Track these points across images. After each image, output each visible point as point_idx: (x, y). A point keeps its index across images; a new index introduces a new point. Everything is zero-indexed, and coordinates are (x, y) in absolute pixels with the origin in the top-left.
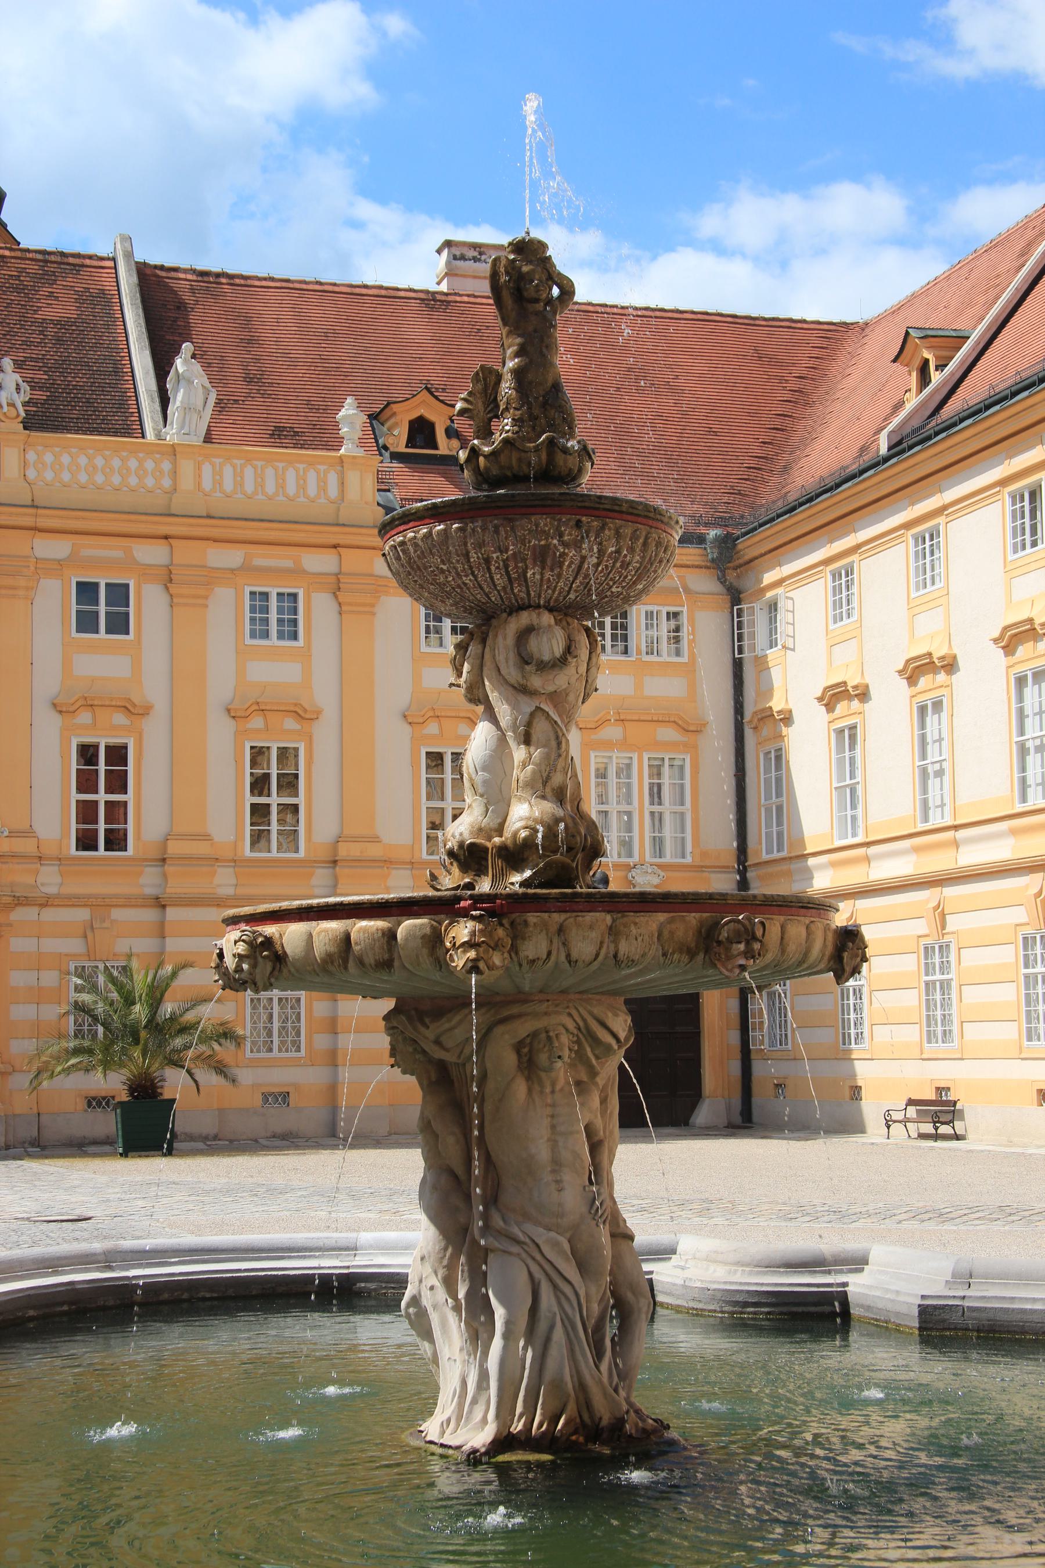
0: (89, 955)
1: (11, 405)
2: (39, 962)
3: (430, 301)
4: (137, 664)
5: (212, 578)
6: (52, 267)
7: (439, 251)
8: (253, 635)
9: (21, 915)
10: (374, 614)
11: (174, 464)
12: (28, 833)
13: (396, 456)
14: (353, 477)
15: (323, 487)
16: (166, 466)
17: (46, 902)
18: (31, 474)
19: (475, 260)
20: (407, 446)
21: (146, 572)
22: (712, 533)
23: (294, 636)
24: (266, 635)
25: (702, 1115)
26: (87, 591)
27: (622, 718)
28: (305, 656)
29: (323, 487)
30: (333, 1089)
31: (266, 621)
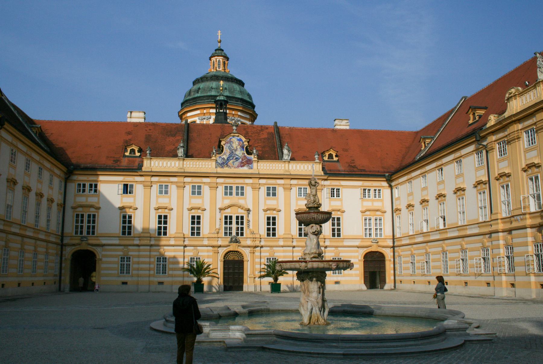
0: (270, 256)
6: (263, 128)
12: (258, 233)
20: (328, 159)
22: (387, 174)
25: (386, 287)
26: (268, 189)
31: (301, 193)
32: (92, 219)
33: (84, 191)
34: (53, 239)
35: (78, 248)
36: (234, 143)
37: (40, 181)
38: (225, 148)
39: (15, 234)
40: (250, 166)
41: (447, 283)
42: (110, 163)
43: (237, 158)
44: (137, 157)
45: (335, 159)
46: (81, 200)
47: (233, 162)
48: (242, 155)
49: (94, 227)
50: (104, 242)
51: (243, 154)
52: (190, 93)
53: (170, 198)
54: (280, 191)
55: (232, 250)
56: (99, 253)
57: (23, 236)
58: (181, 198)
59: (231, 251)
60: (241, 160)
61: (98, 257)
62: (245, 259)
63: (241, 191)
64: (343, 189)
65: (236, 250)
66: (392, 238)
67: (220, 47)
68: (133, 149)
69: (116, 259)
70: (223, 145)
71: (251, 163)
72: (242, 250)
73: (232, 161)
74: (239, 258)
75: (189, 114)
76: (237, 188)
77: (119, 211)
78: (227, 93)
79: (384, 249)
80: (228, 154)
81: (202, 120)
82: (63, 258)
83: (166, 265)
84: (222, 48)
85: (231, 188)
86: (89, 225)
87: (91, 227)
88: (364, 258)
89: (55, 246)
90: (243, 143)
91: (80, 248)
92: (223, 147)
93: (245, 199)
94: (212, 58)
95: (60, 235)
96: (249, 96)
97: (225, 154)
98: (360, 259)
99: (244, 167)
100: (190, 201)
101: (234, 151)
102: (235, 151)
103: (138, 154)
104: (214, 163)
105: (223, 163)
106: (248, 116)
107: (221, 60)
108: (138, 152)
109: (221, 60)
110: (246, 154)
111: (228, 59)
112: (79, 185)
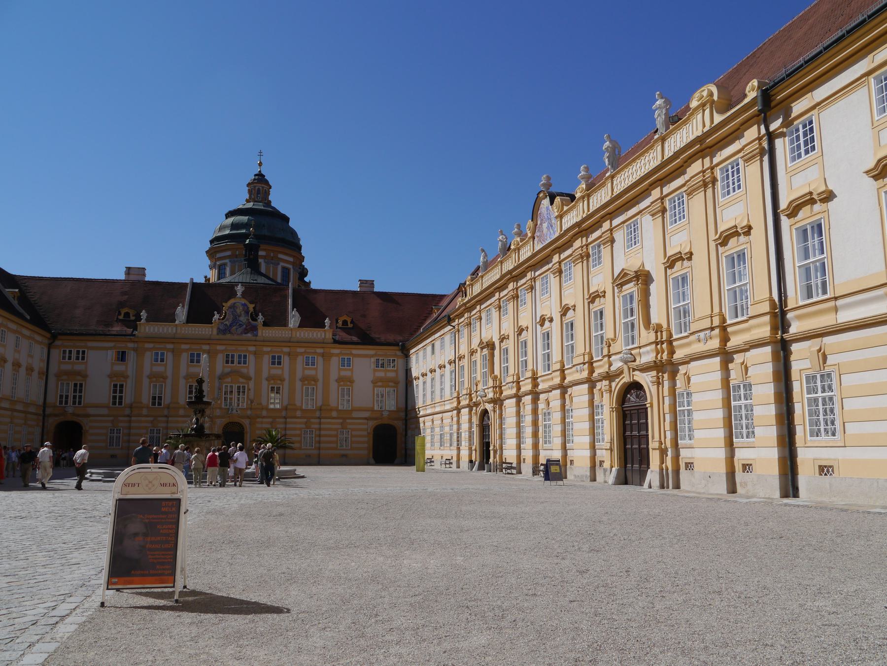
1: (260, 322)
3: (354, 293)
8: (306, 365)
9: (259, 420)
11: (292, 332)
12: (261, 404)
13: (340, 328)
15: (321, 335)
16: (290, 332)
17: (264, 417)
18: (264, 335)
19: (365, 283)
23: (314, 365)
24: (309, 365)
26: (273, 357)
28: (316, 369)
29: (321, 335)
30: (319, 455)
32: (79, 388)
33: (70, 358)
36: (238, 309)
40: (255, 332)
41: (524, 459)
43: (240, 324)
45: (350, 325)
46: (66, 367)
49: (80, 397)
50: (91, 411)
51: (247, 320)
52: (222, 228)
53: (165, 366)
54: (286, 360)
55: (231, 421)
59: (230, 423)
60: (244, 326)
61: (84, 428)
63: (243, 359)
64: (354, 358)
67: (260, 171)
68: (127, 312)
75: (218, 255)
76: (240, 356)
79: (396, 422)
80: (231, 320)
84: (263, 172)
85: (233, 356)
86: (75, 394)
87: (78, 396)
90: (248, 308)
93: (248, 368)
96: (293, 233)
97: (228, 320)
101: (237, 316)
102: (239, 317)
103: (132, 318)
104: (215, 331)
105: (226, 330)
106: (291, 259)
107: (261, 188)
108: (133, 316)
109: (261, 188)
110: (250, 320)
111: (270, 187)
112: (64, 352)
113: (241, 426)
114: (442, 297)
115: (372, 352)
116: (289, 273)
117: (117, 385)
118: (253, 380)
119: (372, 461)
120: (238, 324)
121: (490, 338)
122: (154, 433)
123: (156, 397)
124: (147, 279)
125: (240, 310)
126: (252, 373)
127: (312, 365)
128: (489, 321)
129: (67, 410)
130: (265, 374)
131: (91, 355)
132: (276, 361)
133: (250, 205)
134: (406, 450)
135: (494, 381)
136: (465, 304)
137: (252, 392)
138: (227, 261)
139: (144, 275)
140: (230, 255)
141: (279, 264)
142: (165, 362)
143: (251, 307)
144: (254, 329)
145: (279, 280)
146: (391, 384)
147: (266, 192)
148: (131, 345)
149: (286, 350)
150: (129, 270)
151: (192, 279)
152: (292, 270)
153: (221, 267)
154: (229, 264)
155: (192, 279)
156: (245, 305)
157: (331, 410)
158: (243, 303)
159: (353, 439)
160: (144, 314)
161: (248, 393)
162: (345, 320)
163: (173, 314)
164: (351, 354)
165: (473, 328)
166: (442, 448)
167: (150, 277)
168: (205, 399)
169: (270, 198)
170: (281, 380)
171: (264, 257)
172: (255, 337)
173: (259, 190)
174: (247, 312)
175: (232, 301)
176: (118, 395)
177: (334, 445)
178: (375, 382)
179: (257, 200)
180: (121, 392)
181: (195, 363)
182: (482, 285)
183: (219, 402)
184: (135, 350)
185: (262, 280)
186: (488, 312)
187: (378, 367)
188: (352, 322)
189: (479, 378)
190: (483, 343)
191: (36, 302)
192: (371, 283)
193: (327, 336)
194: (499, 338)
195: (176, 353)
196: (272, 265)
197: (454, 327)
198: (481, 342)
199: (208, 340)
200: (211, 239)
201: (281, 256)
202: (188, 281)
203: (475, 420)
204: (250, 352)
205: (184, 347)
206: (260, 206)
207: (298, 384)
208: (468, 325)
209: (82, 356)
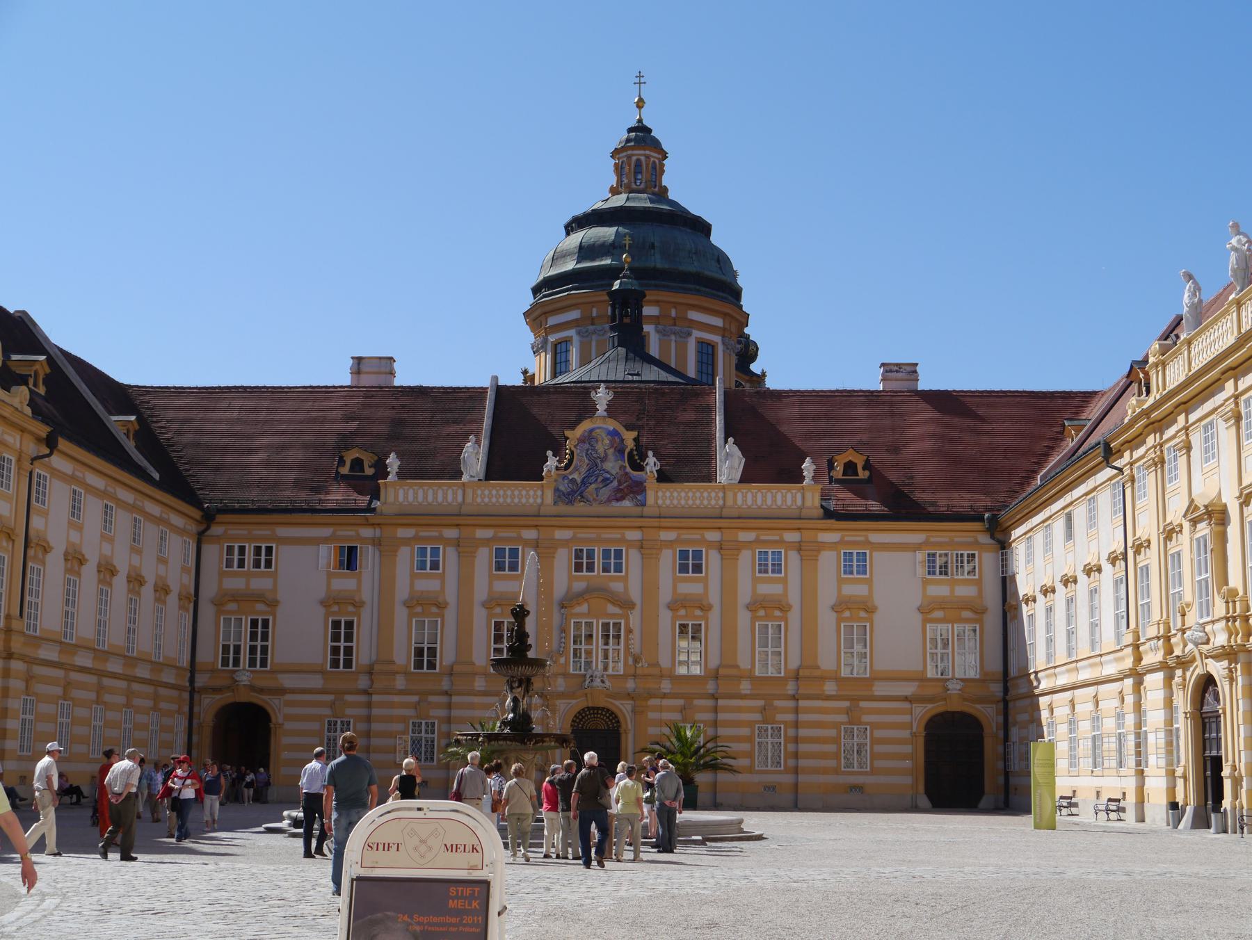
1: (652, 472)
2: (661, 723)
3: (870, 395)
4: (706, 588)
5: (739, 546)
7: (880, 367)
8: (760, 572)
9: (654, 702)
10: (817, 560)
12: (657, 665)
13: (838, 481)
14: (808, 495)
16: (721, 495)
17: (664, 696)
19: (897, 371)
21: (710, 545)
23: (780, 572)
24: (766, 572)
25: (982, 804)
26: (684, 555)
27: (942, 607)
28: (784, 581)
29: (794, 499)
30: (796, 785)
32: (260, 629)
33: (241, 564)
34: (168, 677)
35: (227, 698)
36: (600, 442)
37: (136, 550)
38: (578, 455)
39: (83, 670)
42: (303, 497)
43: (605, 480)
44: (368, 477)
45: (863, 474)
47: (596, 489)
48: (618, 470)
49: (264, 650)
50: (287, 681)
52: (557, 258)
53: (442, 577)
54: (712, 561)
55: (590, 705)
56: (277, 711)
57: (101, 674)
58: (465, 582)
60: (615, 483)
61: (273, 720)
62: (622, 730)
63: (614, 560)
64: (877, 556)
65: (601, 705)
66: (1000, 677)
67: (640, 121)
69: (315, 726)
70: (573, 449)
71: (642, 491)
72: (614, 705)
73: (593, 486)
74: (608, 726)
75: (553, 320)
76: (606, 553)
77: (322, 610)
78: (657, 261)
79: (978, 706)
80: (584, 469)
81: (587, 336)
82: (195, 721)
83: (433, 741)
85: (590, 554)
88: (925, 730)
89: (174, 693)
90: (622, 440)
91: (231, 700)
92: (572, 453)
94: (619, 154)
95: (189, 668)
96: (721, 260)
97: (576, 469)
98: (914, 730)
99: (624, 501)
100: (490, 585)
101: (599, 461)
102: (602, 461)
103: (369, 471)
104: (549, 496)
105: (573, 492)
106: (718, 322)
108: (370, 467)
109: (643, 158)
110: (629, 469)
112: (230, 550)
113: (612, 716)
114: (1086, 397)
115: (918, 538)
116: (713, 355)
117: (340, 622)
118: (638, 607)
119: (924, 801)
120: (600, 479)
121: (1213, 494)
122: (420, 732)
123: (423, 648)
124: (399, 381)
125: (603, 445)
126: (635, 594)
127: (773, 571)
128: (1210, 451)
129: (238, 679)
130: (665, 595)
131: (285, 556)
132: (691, 564)
133: (620, 201)
134: (1007, 774)
135: (1227, 602)
136: (1146, 413)
137: (636, 636)
138: (572, 333)
139: (392, 373)
140: (577, 320)
141: (689, 334)
142: (440, 571)
143: (629, 437)
144: (636, 489)
145: (692, 372)
146: (966, 614)
147: (654, 168)
148: (367, 532)
149: (713, 536)
150: (359, 364)
151: (495, 378)
152: (720, 349)
153: (559, 346)
154: (576, 340)
155: (495, 378)
156: (615, 433)
157: (823, 678)
158: (611, 428)
159: (879, 748)
160: (393, 462)
161: (627, 639)
162: (850, 461)
163: (456, 461)
164: (867, 543)
165: (1170, 470)
166: (1098, 771)
167: (403, 378)
168: (531, 654)
169: (666, 181)
170: (701, 609)
171: (655, 320)
172: (639, 509)
173: (638, 161)
174: (620, 451)
175: (585, 426)
176: (342, 644)
177: (831, 763)
178: (927, 610)
179: (634, 186)
180: (349, 638)
181: (507, 572)
182: (1190, 364)
183: (562, 660)
184: (377, 542)
185: (651, 374)
186: (1206, 431)
187: (934, 573)
188: (867, 466)
189: (1188, 597)
190: (1197, 508)
191: (171, 442)
192: (911, 370)
193: (808, 503)
194: (1237, 495)
195: (465, 548)
196: (673, 337)
197: (1121, 470)
198: (1192, 506)
199: (533, 518)
200: (534, 281)
201: (694, 315)
202: (485, 382)
203: (1183, 702)
204: (630, 544)
205: (481, 533)
206: (642, 201)
207: (744, 617)
208: (1156, 465)
209: (265, 558)
